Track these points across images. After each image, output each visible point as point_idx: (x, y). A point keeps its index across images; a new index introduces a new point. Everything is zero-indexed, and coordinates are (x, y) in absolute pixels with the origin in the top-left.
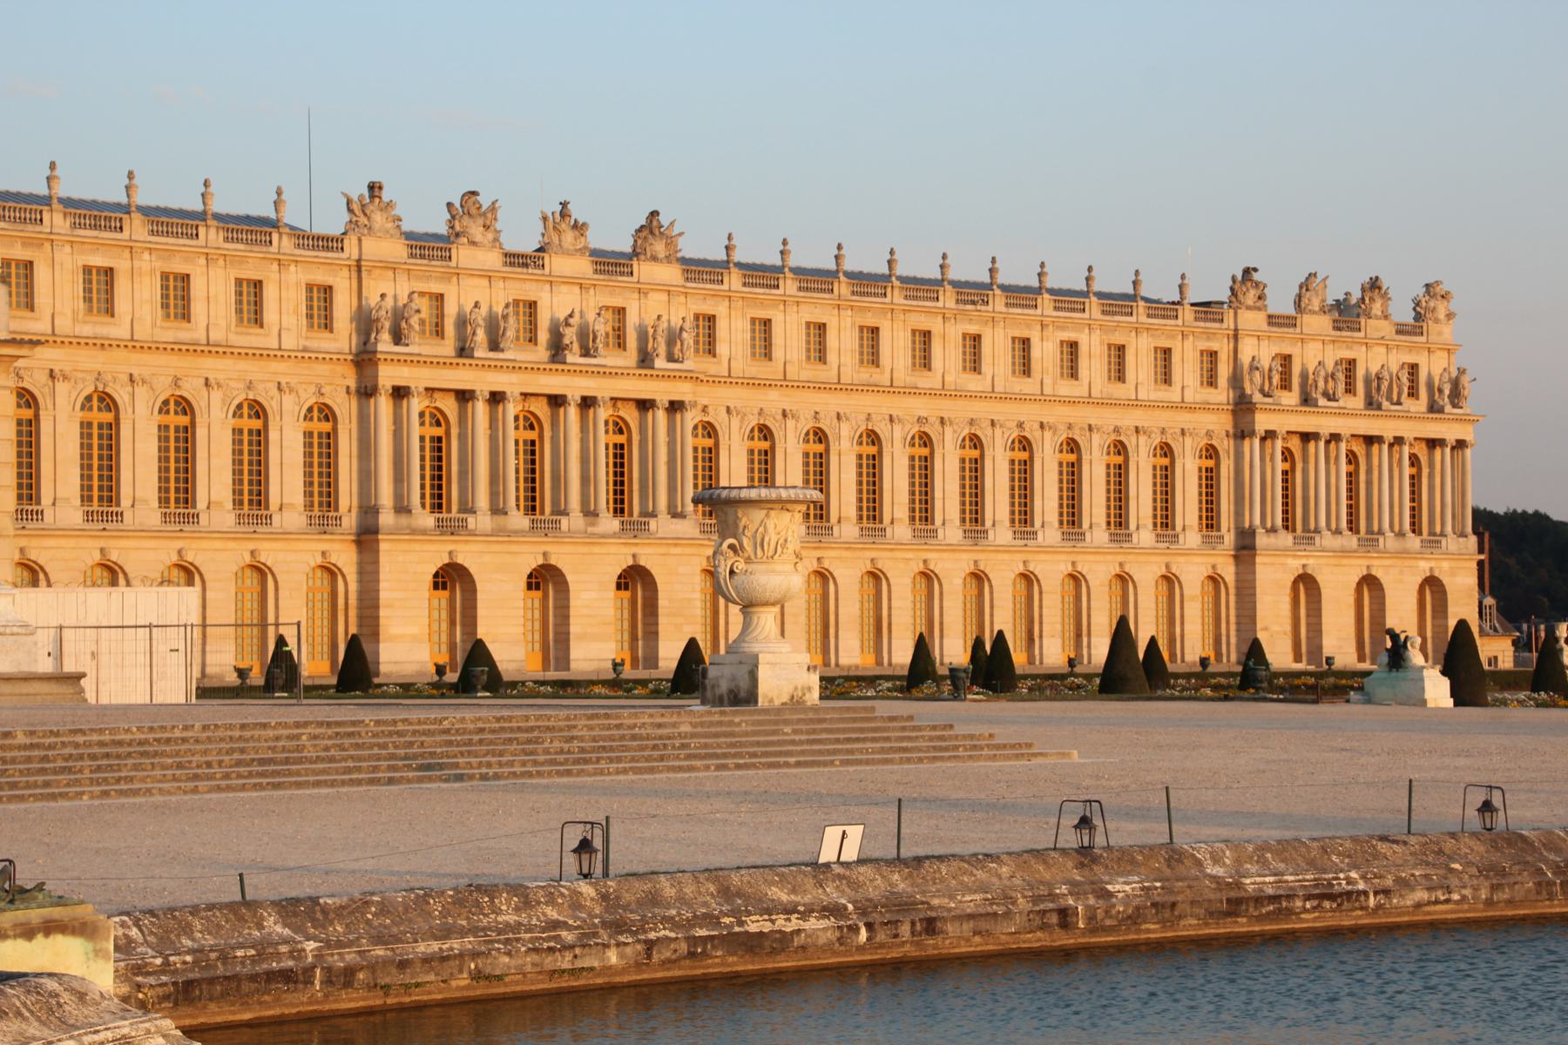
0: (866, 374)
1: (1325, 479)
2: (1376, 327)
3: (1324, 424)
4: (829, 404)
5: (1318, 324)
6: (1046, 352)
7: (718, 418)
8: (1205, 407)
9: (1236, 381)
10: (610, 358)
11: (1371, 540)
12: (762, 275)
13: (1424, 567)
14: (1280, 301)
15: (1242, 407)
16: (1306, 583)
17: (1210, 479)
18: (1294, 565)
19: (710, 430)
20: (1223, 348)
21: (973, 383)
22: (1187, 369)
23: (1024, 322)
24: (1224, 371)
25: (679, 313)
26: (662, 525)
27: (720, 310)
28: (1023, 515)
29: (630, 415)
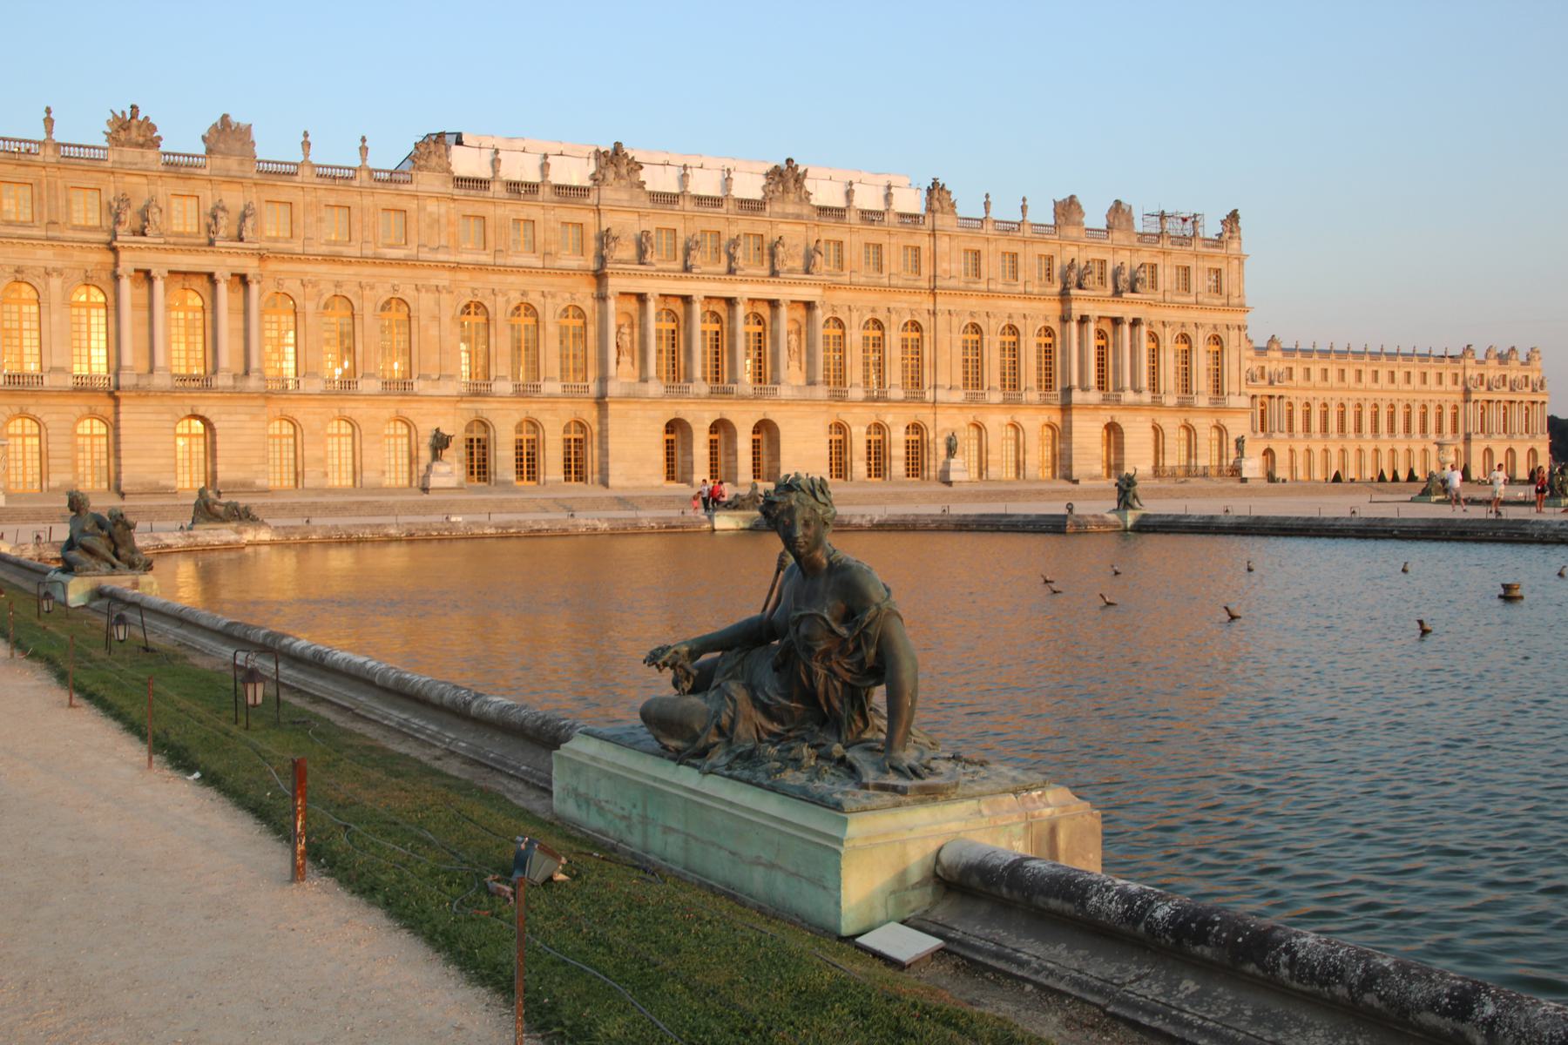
0: (1341, 385)
1: (1495, 415)
2: (1514, 363)
3: (1495, 397)
4: (1328, 395)
5: (1493, 363)
6: (1399, 375)
7: (1293, 400)
8: (1454, 392)
9: (1465, 383)
10: (1260, 382)
11: (1511, 436)
12: (1307, 353)
13: (1530, 445)
14: (1480, 356)
15: (1467, 392)
16: (1488, 451)
17: (1455, 416)
18: (1485, 445)
19: (1290, 404)
20: (1460, 372)
21: (1376, 387)
22: (1447, 380)
23: (1392, 365)
24: (1460, 380)
25: (1281, 368)
26: (1277, 435)
27: (1294, 365)
28: (1392, 429)
29: (1266, 400)
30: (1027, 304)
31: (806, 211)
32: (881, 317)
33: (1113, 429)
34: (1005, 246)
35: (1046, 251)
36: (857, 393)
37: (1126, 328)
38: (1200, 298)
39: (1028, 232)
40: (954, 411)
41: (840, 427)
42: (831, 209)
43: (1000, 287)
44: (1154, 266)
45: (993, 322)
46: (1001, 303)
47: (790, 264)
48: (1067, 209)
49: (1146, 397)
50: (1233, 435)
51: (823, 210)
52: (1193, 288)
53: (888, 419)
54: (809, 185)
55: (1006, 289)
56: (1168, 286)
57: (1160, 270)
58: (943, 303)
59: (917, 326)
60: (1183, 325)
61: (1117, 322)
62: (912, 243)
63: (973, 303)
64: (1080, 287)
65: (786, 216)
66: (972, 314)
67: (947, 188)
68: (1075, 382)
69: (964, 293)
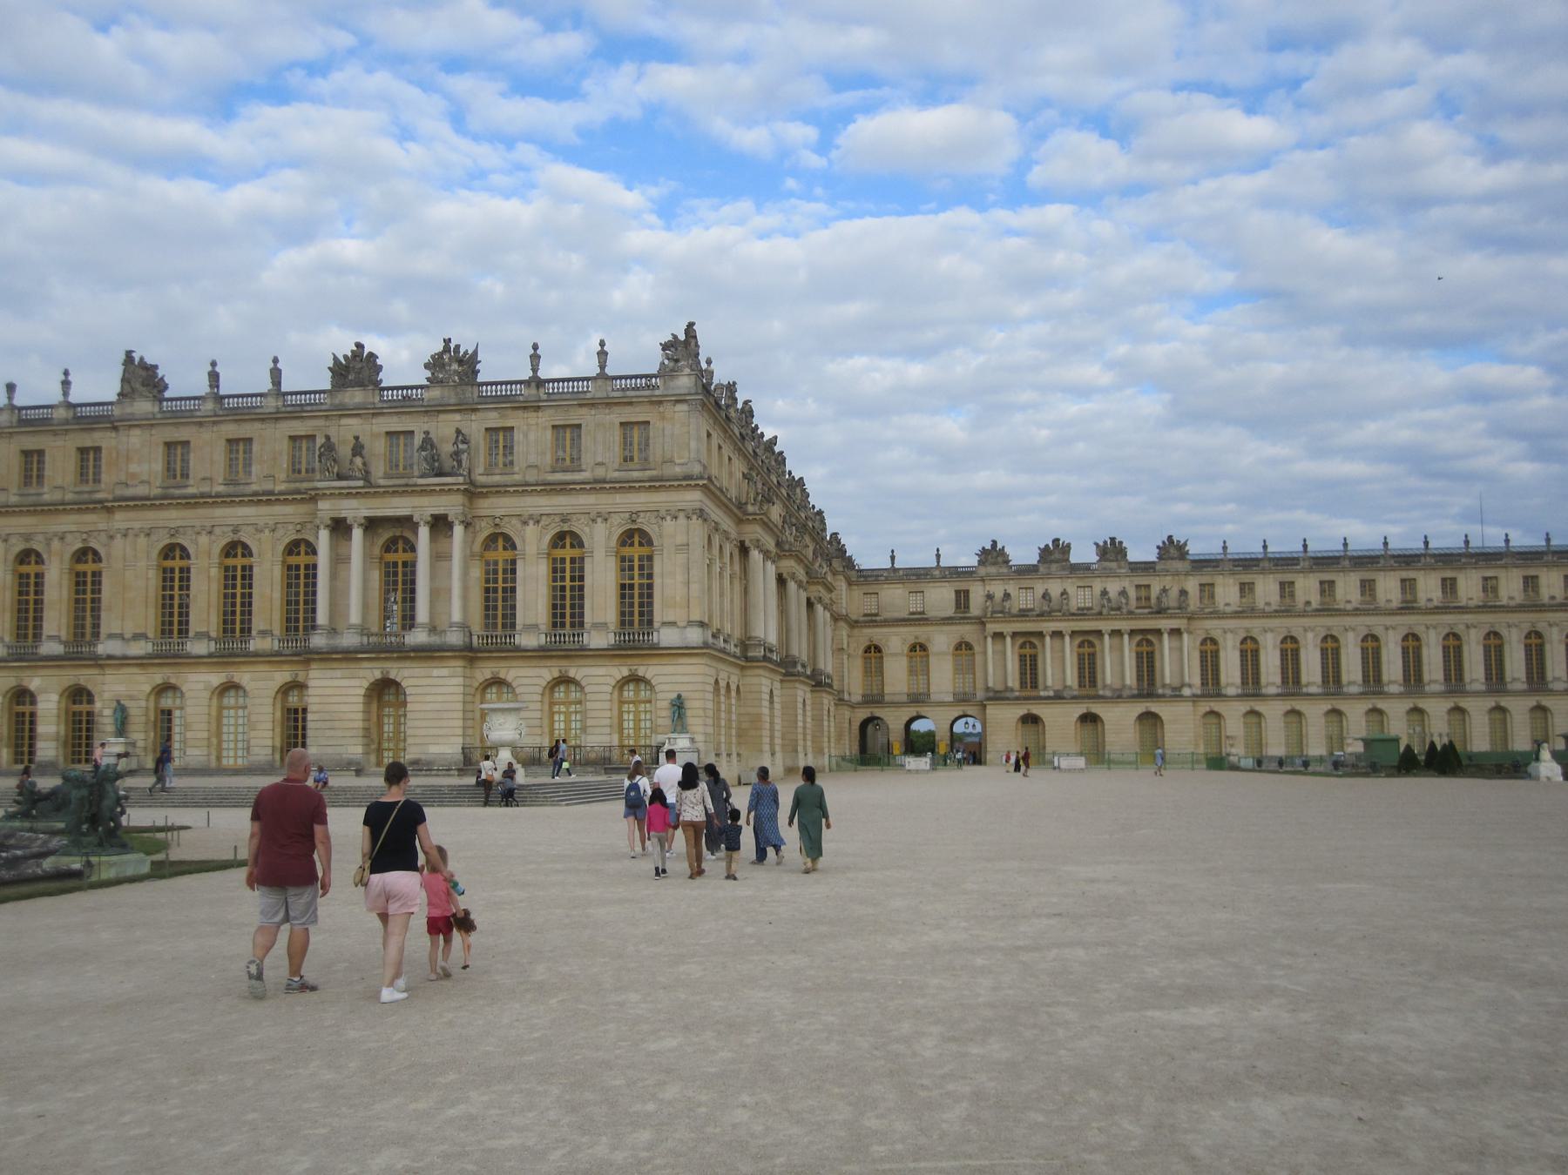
30: (264, 510)
33: (385, 691)
34: (232, 430)
35: (300, 428)
37: (424, 532)
38: (600, 472)
39: (271, 404)
40: (136, 670)
43: (221, 489)
45: (204, 539)
46: (219, 512)
48: (356, 370)
50: (665, 695)
52: (587, 459)
53: (34, 683)
55: (231, 489)
56: (533, 459)
57: (518, 436)
58: (121, 520)
60: (565, 519)
61: (407, 522)
62: (88, 443)
67: (149, 361)
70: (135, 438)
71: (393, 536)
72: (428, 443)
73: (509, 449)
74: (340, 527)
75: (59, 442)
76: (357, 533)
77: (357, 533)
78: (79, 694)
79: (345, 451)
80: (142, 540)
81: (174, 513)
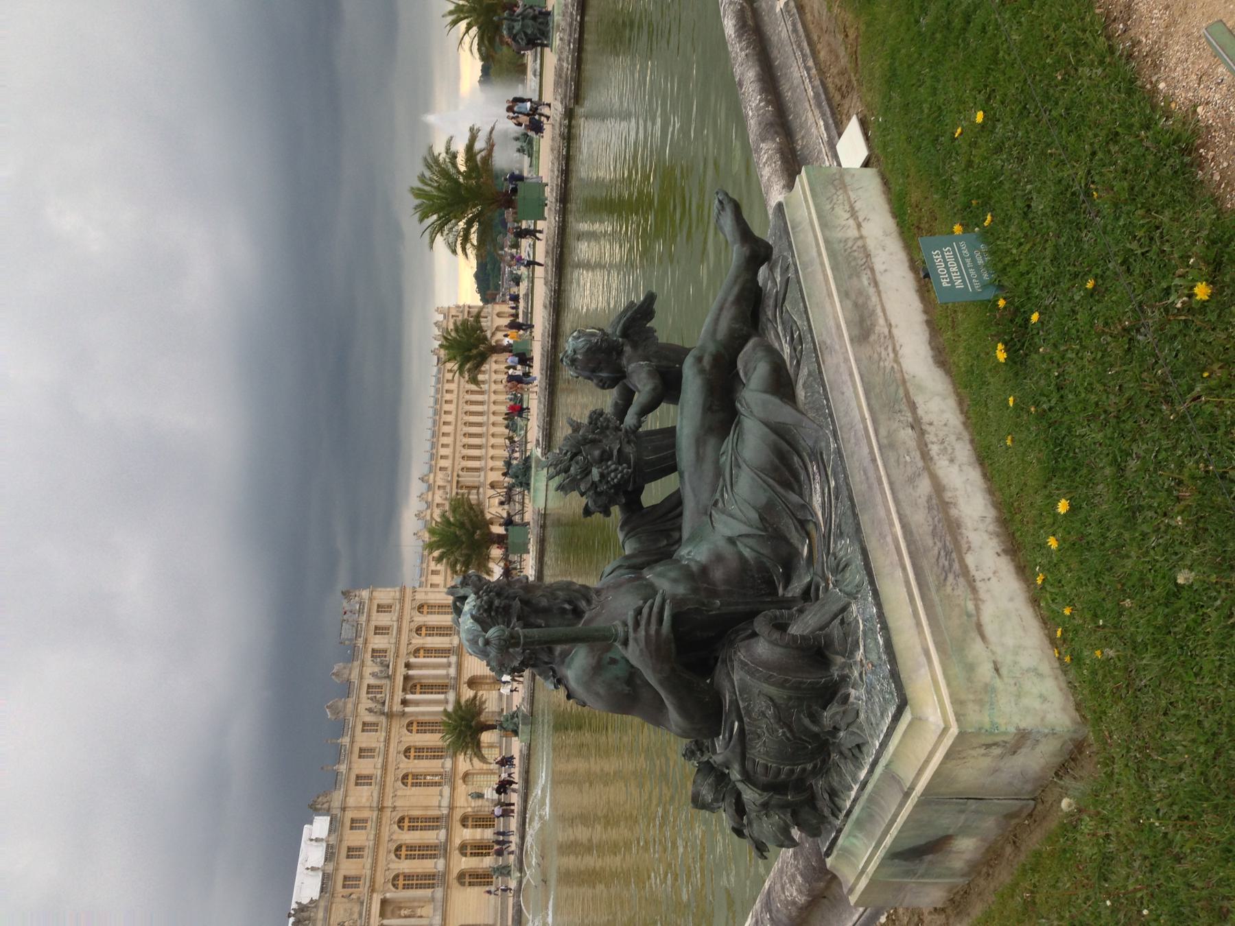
31: (322, 904)
32: (393, 846)
35: (359, 727)
36: (441, 864)
37: (411, 672)
38: (395, 618)
41: (461, 876)
42: (323, 884)
43: (380, 760)
44: (373, 651)
45: (401, 766)
46: (390, 759)
47: (356, 916)
49: (453, 659)
51: (322, 890)
52: (389, 623)
53: (457, 842)
54: (305, 901)
57: (376, 647)
58: (388, 803)
59: (401, 820)
60: (411, 631)
62: (348, 823)
63: (390, 779)
64: (384, 703)
65: (325, 919)
66: (396, 781)
68: (441, 709)
69: (383, 787)
70: (351, 801)
71: (410, 684)
72: (374, 675)
73: (380, 651)
74: (404, 702)
75: (345, 837)
76: (409, 697)
77: (409, 697)
78: (464, 821)
79: (371, 705)
80: (399, 793)
81: (388, 779)
